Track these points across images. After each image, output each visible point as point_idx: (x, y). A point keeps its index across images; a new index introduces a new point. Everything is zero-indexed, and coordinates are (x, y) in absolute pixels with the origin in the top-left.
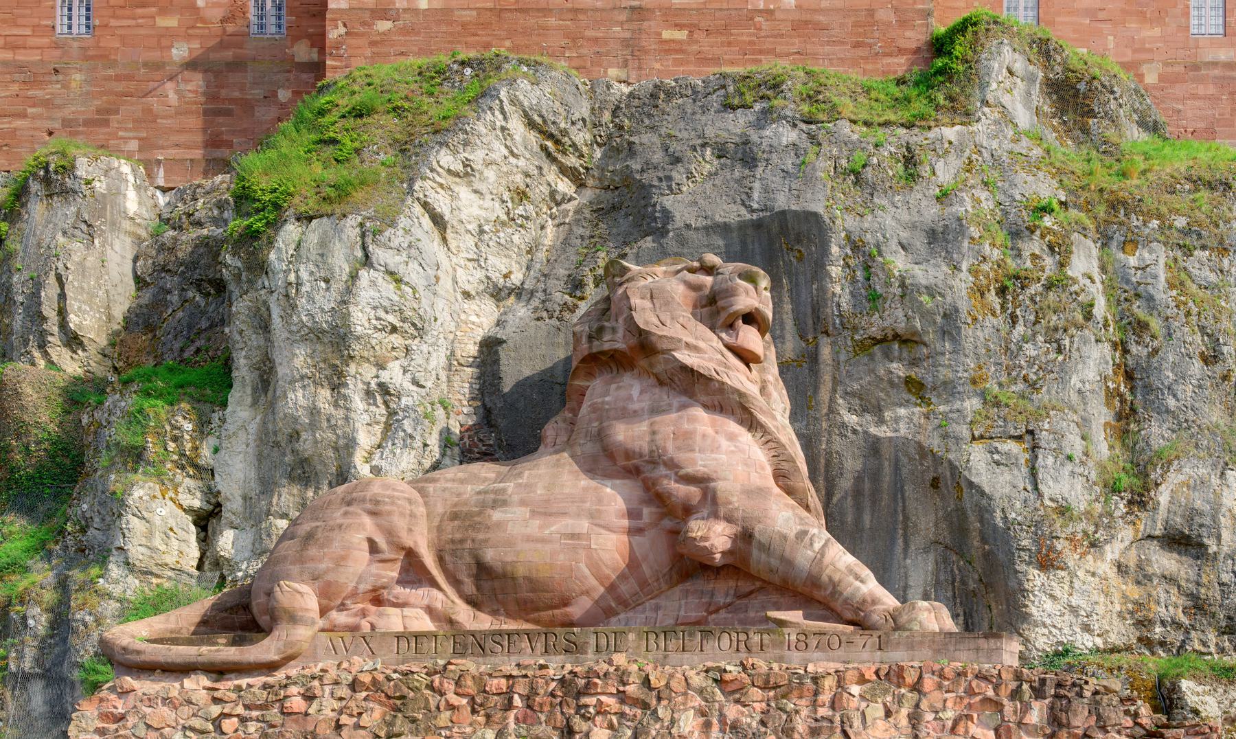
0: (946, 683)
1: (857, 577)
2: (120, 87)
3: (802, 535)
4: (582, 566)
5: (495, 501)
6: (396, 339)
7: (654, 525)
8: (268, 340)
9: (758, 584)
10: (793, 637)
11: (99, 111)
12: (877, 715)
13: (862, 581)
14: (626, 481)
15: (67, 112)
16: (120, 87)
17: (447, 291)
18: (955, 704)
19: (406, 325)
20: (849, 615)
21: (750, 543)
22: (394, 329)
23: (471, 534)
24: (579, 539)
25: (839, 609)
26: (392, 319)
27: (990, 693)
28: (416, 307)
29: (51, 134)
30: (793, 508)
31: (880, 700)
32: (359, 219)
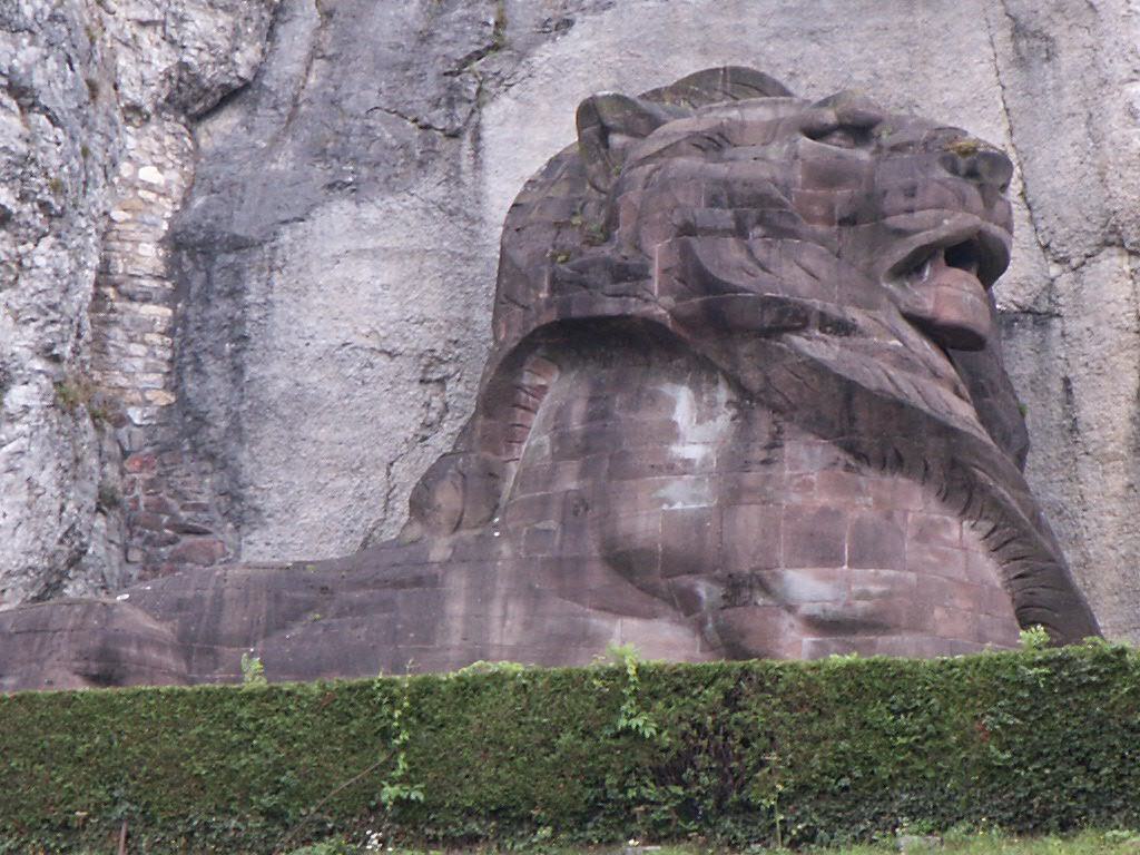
19: (27, 208)
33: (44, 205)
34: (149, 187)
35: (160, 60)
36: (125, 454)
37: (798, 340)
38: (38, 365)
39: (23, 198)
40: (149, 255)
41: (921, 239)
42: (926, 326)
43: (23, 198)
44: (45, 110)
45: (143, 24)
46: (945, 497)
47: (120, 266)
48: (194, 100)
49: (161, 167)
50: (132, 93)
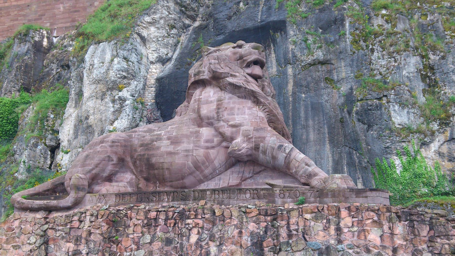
0: (353, 213)
1: (307, 164)
2: (47, 7)
3: (280, 147)
4: (190, 163)
5: (157, 138)
6: (125, 81)
7: (219, 144)
8: (82, 84)
9: (263, 168)
10: (278, 192)
11: (39, 16)
12: (319, 229)
13: (309, 166)
14: (208, 128)
15: (30, 18)
16: (47, 7)
17: (145, 62)
18: (358, 223)
19: (129, 75)
20: (303, 181)
21: (258, 151)
22: (125, 77)
23: (147, 152)
24: (189, 152)
25: (299, 178)
26: (124, 74)
27: (376, 218)
28: (133, 69)
29: (24, 24)
30: (276, 135)
31: (320, 222)
32: (116, 41)
33: (132, 75)
34: (154, 72)
35: (156, 55)
36: (148, 109)
37: (227, 79)
38: (131, 97)
39: (128, 74)
40: (153, 81)
41: (249, 60)
42: (250, 75)
43: (128, 74)
44: (130, 61)
45: (153, 51)
46: (254, 102)
47: (148, 83)
48: (163, 61)
49: (156, 69)
50: (151, 60)
